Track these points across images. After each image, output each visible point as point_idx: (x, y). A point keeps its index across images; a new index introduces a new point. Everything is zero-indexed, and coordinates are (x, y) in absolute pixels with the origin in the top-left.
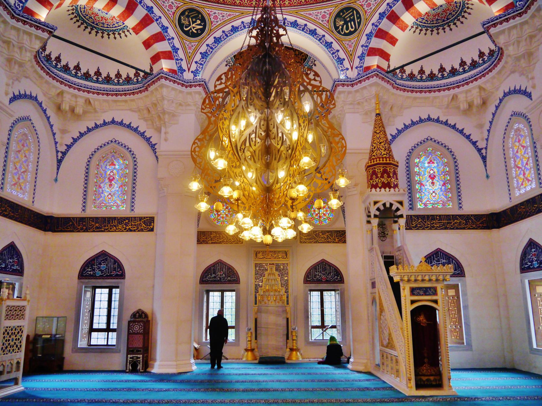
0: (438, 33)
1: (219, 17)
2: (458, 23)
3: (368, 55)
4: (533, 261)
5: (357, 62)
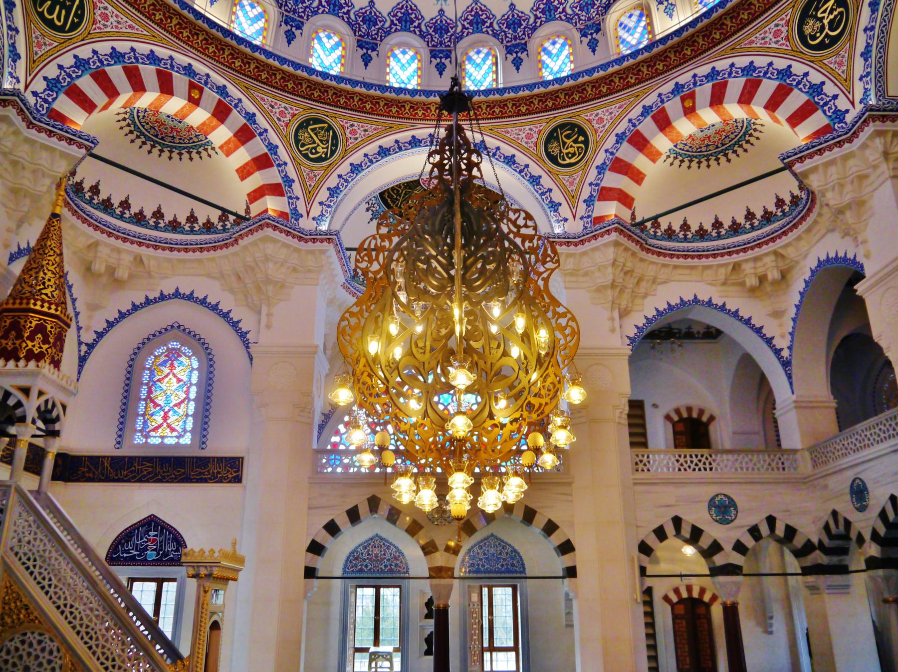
0: (132, 141)
2: (166, 154)
3: (67, 93)
4: (146, 549)
5: (39, 85)
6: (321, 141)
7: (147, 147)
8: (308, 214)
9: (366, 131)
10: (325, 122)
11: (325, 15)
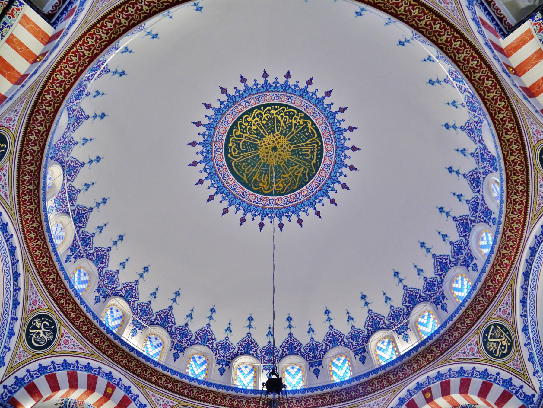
6: (500, 338)
8: (534, 390)
9: (507, 303)
10: (490, 327)
11: (446, 276)
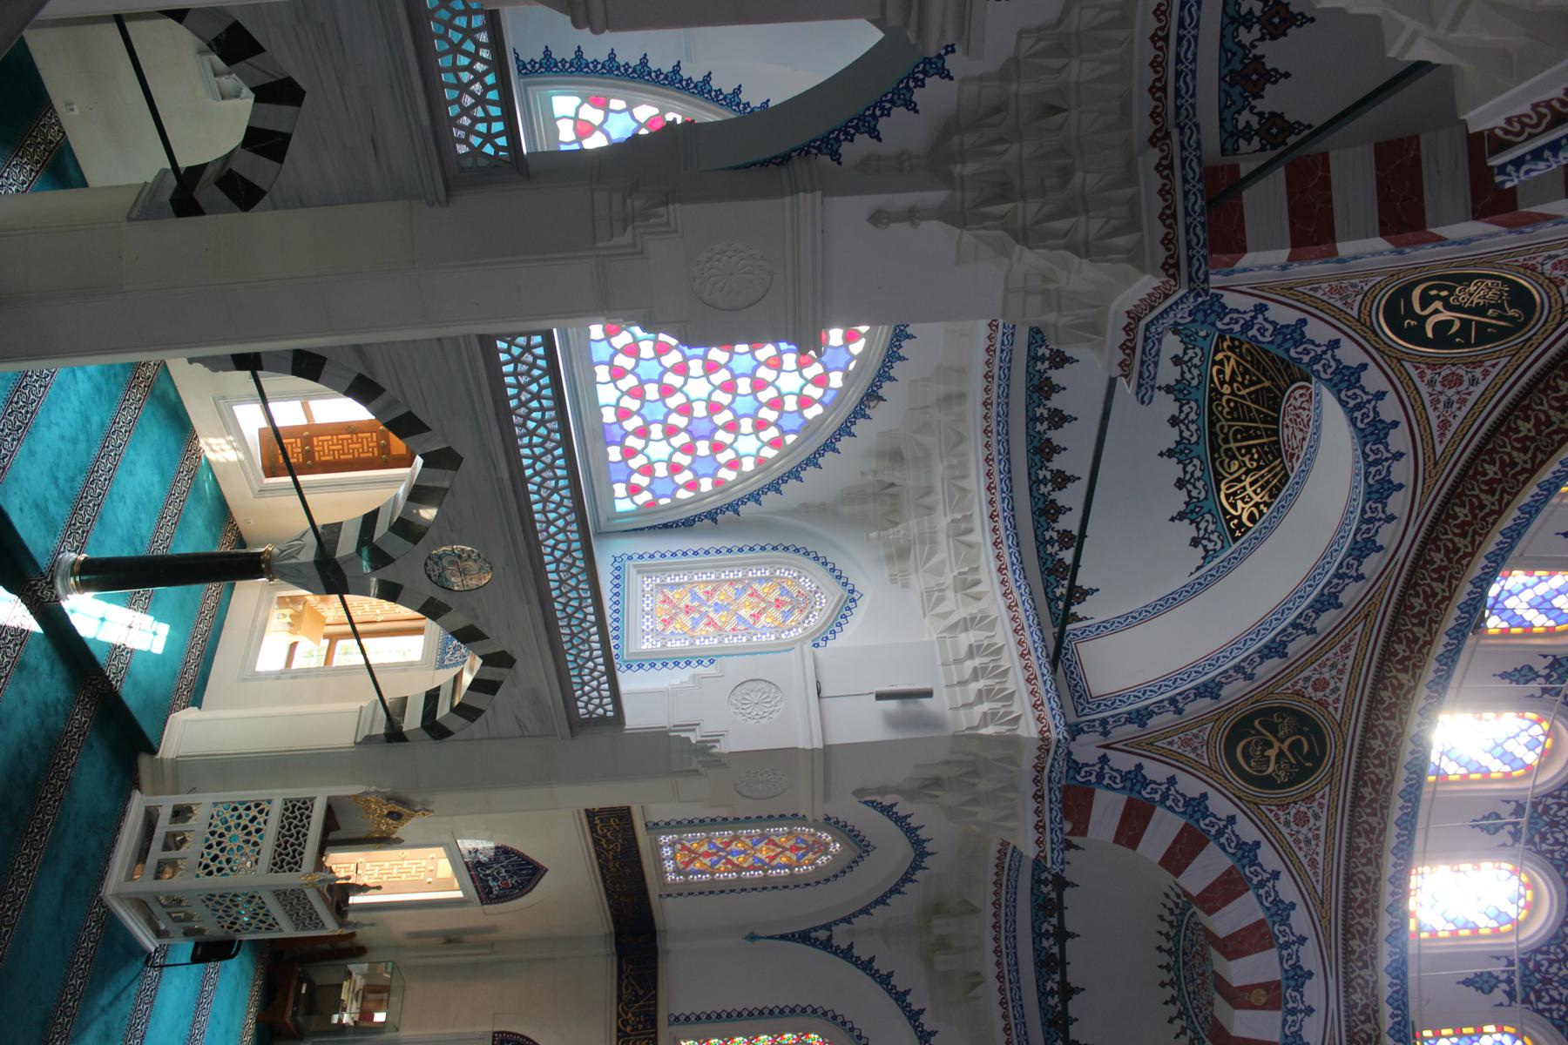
0: (1161, 917)
1: (1450, 392)
2: (1166, 976)
7: (1167, 945)
